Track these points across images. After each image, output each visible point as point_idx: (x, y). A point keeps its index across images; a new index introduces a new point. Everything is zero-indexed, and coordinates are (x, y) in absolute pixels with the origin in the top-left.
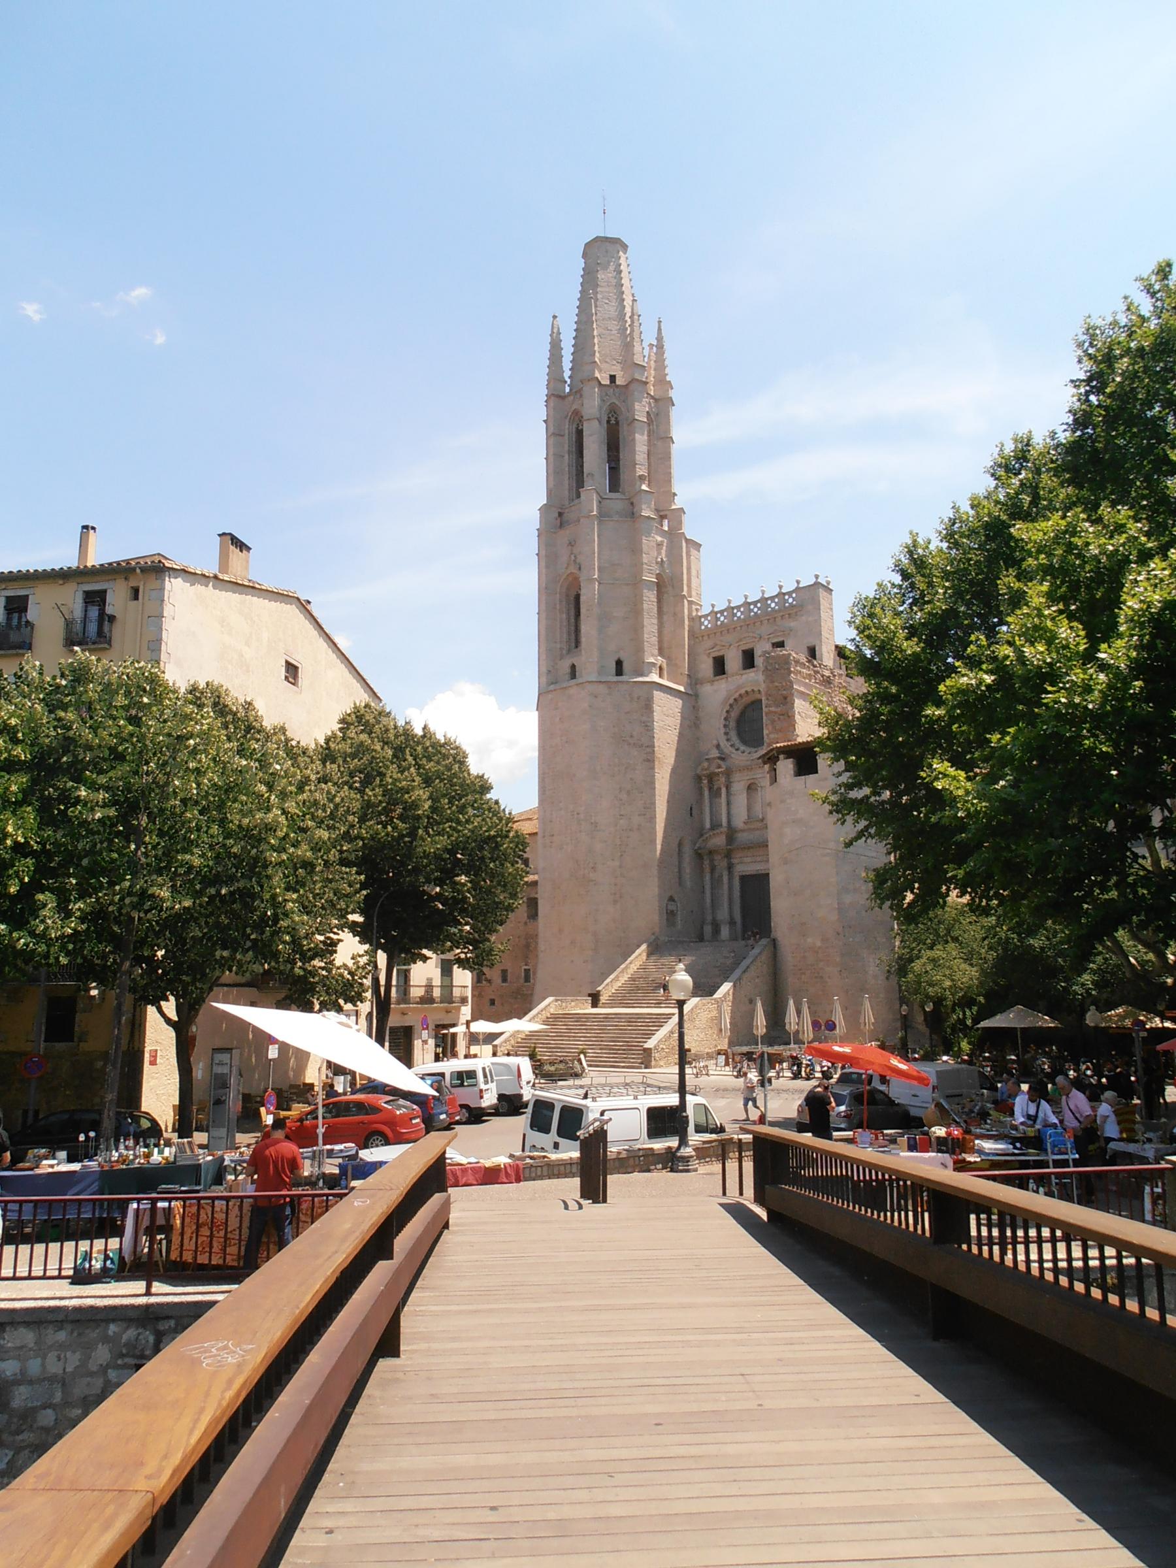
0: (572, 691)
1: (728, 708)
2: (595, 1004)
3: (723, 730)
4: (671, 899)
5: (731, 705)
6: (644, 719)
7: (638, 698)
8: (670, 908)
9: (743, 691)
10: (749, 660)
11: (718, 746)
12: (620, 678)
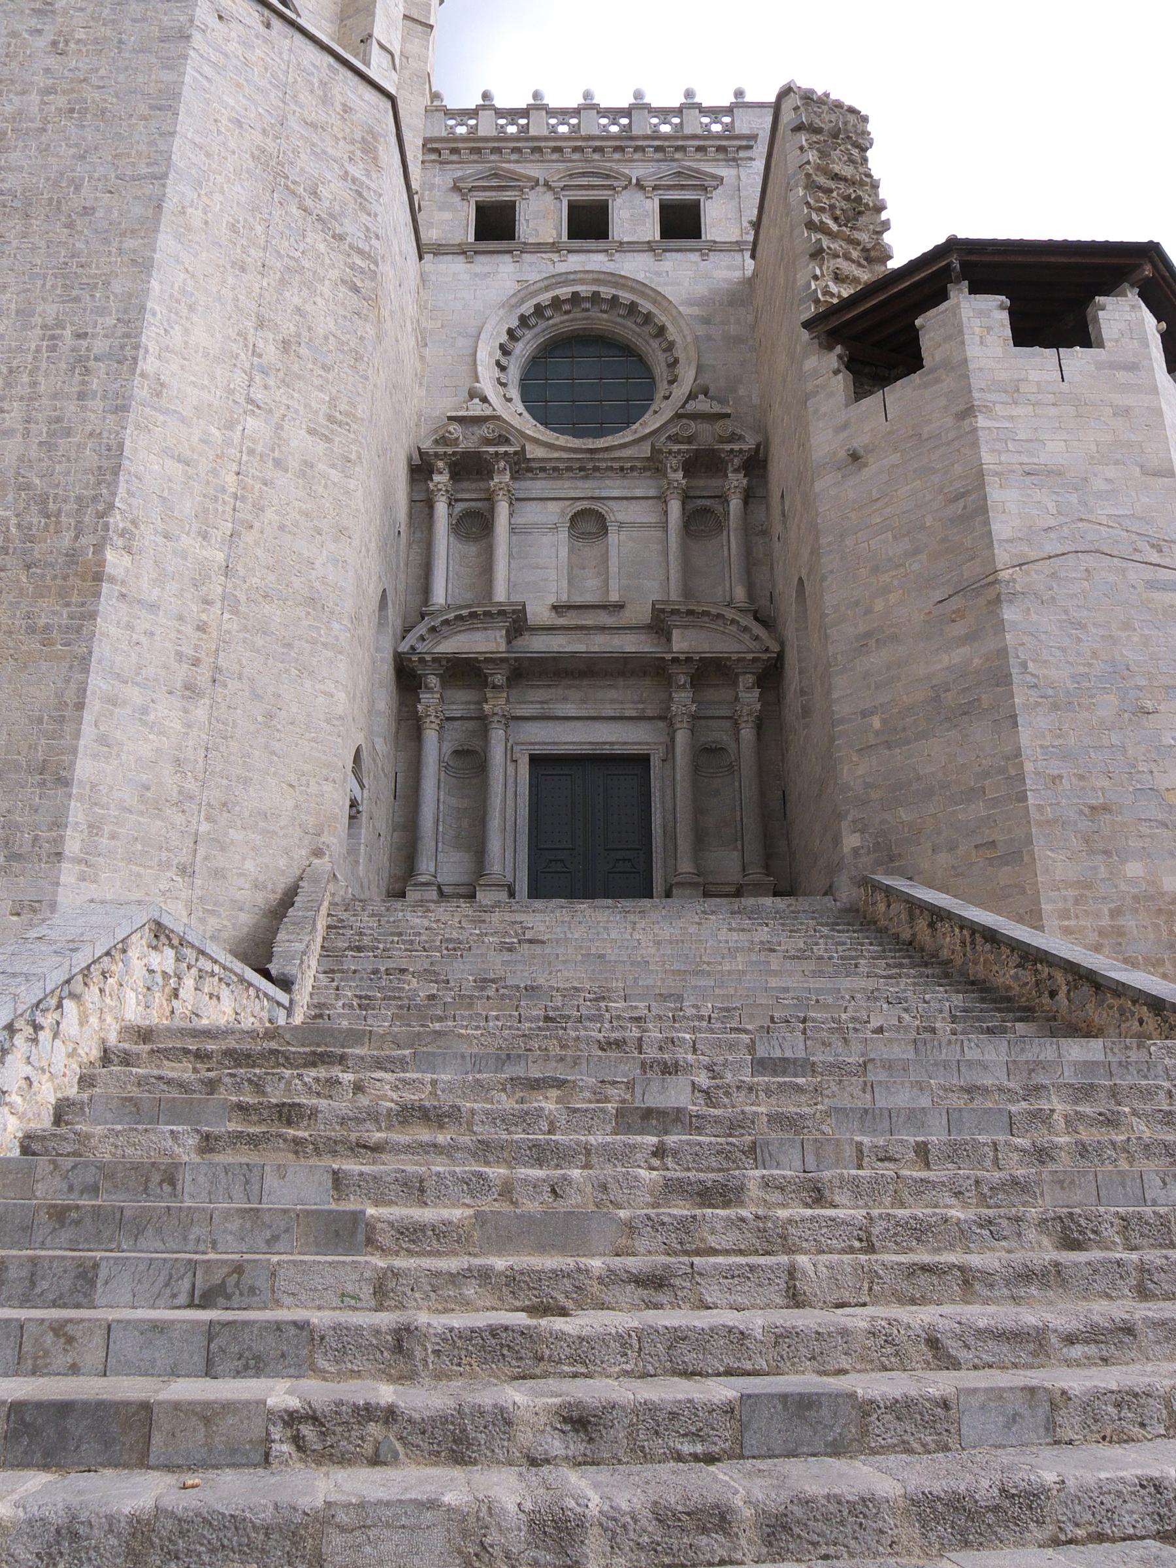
6: (355, 171)
9: (564, 292)
10: (588, 223)
11: (484, 400)
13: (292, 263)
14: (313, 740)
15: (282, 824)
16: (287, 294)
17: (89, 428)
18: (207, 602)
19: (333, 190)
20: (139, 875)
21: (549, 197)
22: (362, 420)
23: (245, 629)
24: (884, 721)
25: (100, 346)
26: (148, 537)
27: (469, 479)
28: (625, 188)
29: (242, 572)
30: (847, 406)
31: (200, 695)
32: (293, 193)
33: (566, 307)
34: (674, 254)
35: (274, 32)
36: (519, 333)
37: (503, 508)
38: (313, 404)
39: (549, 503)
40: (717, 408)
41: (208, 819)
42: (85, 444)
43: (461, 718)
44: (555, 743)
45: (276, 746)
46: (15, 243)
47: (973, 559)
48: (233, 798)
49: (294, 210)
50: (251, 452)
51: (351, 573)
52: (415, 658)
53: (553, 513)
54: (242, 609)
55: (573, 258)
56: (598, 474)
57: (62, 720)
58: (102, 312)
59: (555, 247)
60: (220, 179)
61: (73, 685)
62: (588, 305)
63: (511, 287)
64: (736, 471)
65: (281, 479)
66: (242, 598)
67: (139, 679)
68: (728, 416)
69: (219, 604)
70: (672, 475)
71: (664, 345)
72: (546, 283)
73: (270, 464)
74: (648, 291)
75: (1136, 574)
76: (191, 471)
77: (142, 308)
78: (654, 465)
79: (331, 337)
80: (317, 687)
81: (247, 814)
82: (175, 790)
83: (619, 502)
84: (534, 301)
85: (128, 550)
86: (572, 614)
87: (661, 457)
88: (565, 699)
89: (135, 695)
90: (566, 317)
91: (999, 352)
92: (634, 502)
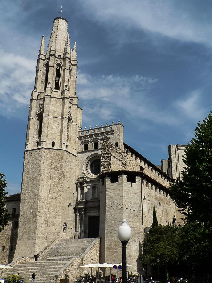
1: (88, 161)
2: (36, 260)
4: (65, 223)
6: (60, 162)
8: (64, 226)
11: (84, 173)
12: (53, 148)
19: (58, 165)
26: (41, 211)
32: (53, 169)
37: (85, 188)
38: (56, 191)
41: (48, 234)
45: (54, 226)
50: (50, 199)
58: (36, 190)
65: (53, 200)
66: (50, 213)
75: (118, 208)
77: (39, 189)
84: (90, 158)
88: (91, 210)
89: (41, 225)
91: (108, 184)
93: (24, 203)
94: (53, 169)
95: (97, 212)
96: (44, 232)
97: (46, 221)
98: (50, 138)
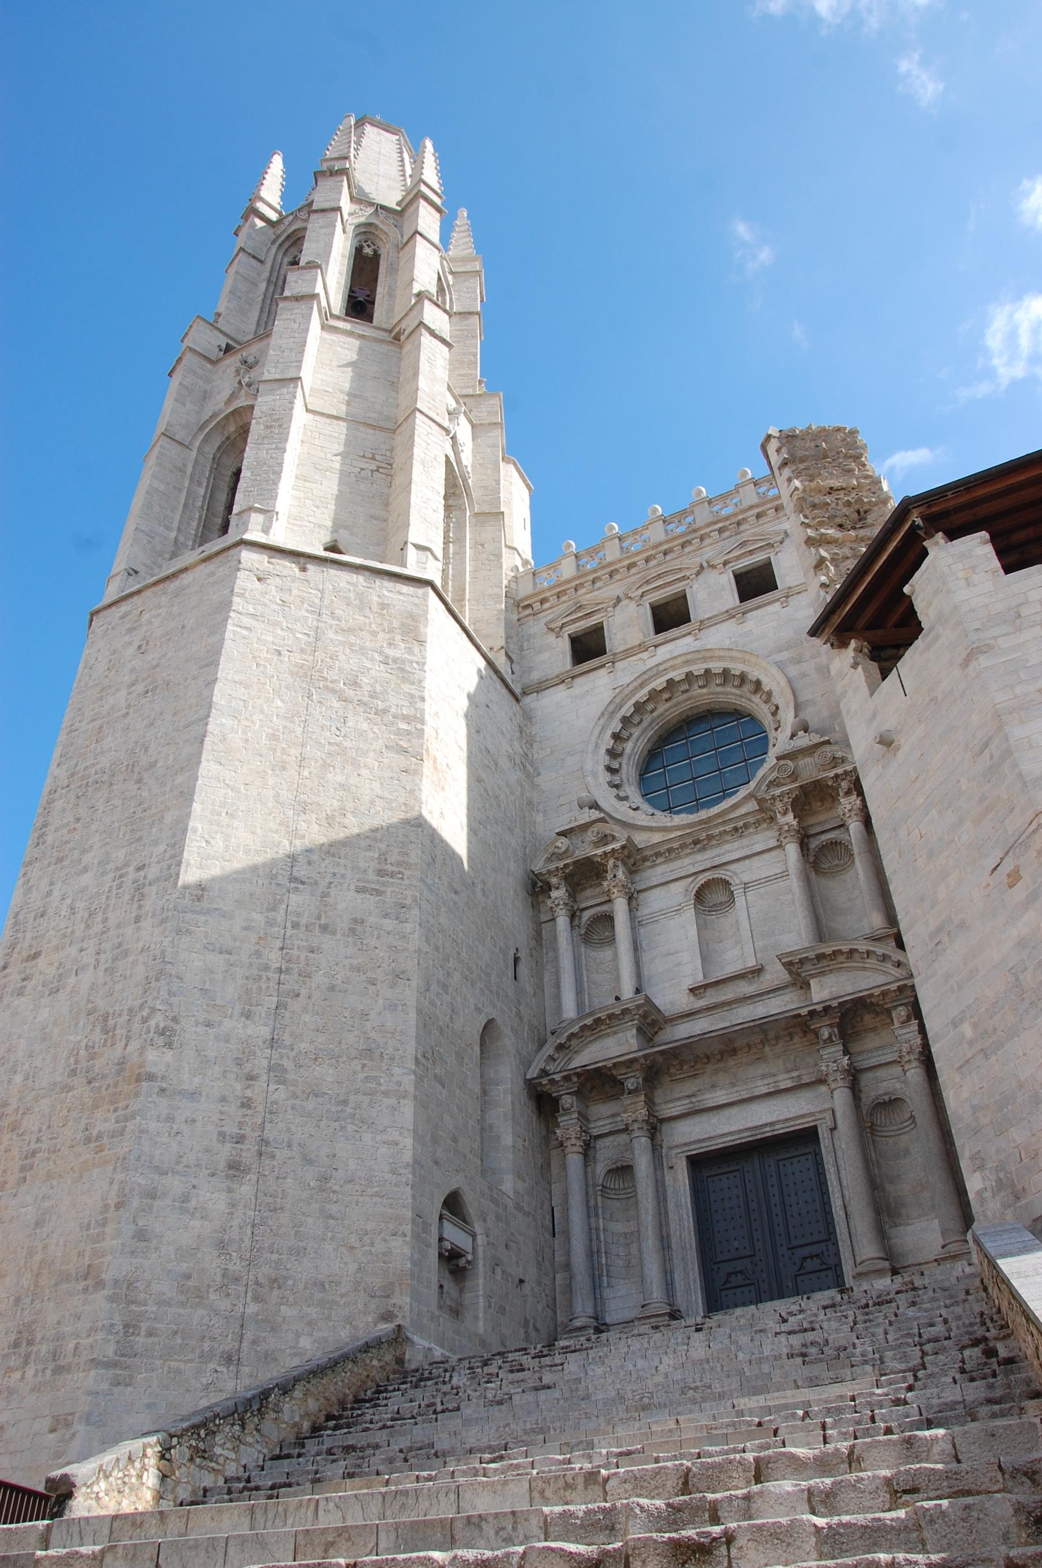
0: (186, 579)
1: (616, 726)
3: (604, 777)
5: (626, 721)
7: (383, 606)
9: (659, 683)
10: (670, 616)
11: (595, 806)
13: (333, 748)
14: (377, 1194)
15: (343, 1291)
16: (330, 776)
17: (141, 945)
18: (251, 1078)
20: (179, 1371)
21: (632, 605)
22: (416, 864)
23: (294, 1096)
24: (975, 1026)
25: (152, 872)
27: (591, 886)
28: (698, 574)
29: (287, 1039)
30: (871, 695)
31: (247, 1171)
32: (334, 691)
33: (666, 696)
34: (754, 613)
35: (309, 573)
36: (625, 734)
38: (362, 865)
39: (672, 886)
40: (816, 739)
41: (257, 1299)
42: (138, 960)
43: (611, 1133)
44: (710, 1138)
45: (333, 1209)
46: (101, 809)
47: (1012, 810)
48: (284, 1273)
49: (335, 704)
50: (295, 925)
51: (413, 1015)
52: (544, 1081)
53: (679, 894)
54: (291, 1076)
55: (661, 650)
56: (714, 842)
57: (104, 1223)
59: (642, 648)
60: (259, 702)
61: (115, 1187)
62: (685, 687)
63: (607, 696)
64: (848, 793)
65: (327, 942)
66: (288, 1064)
67: (180, 1168)
68: (828, 742)
69: (264, 1077)
70: (782, 820)
71: (764, 697)
72: (639, 681)
73: (317, 931)
74: (734, 654)
76: (233, 958)
78: (766, 815)
79: (377, 799)
80: (378, 1138)
81: (301, 1286)
82: (219, 1274)
83: (742, 863)
84: (633, 701)
85: (169, 1045)
86: (710, 992)
87: (768, 805)
89: (175, 1185)
90: (669, 704)
92: (756, 858)
93: (20, 993)
94: (334, 691)
95: (783, 1086)
96: (212, 1263)
97: (240, 1139)
98: (311, 519)
